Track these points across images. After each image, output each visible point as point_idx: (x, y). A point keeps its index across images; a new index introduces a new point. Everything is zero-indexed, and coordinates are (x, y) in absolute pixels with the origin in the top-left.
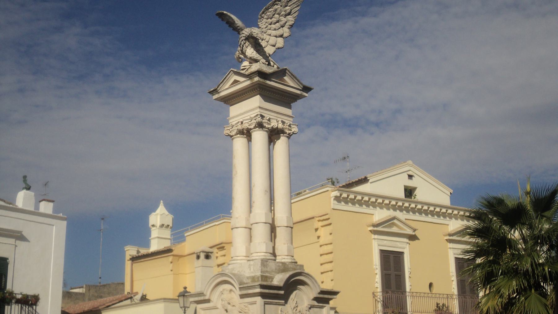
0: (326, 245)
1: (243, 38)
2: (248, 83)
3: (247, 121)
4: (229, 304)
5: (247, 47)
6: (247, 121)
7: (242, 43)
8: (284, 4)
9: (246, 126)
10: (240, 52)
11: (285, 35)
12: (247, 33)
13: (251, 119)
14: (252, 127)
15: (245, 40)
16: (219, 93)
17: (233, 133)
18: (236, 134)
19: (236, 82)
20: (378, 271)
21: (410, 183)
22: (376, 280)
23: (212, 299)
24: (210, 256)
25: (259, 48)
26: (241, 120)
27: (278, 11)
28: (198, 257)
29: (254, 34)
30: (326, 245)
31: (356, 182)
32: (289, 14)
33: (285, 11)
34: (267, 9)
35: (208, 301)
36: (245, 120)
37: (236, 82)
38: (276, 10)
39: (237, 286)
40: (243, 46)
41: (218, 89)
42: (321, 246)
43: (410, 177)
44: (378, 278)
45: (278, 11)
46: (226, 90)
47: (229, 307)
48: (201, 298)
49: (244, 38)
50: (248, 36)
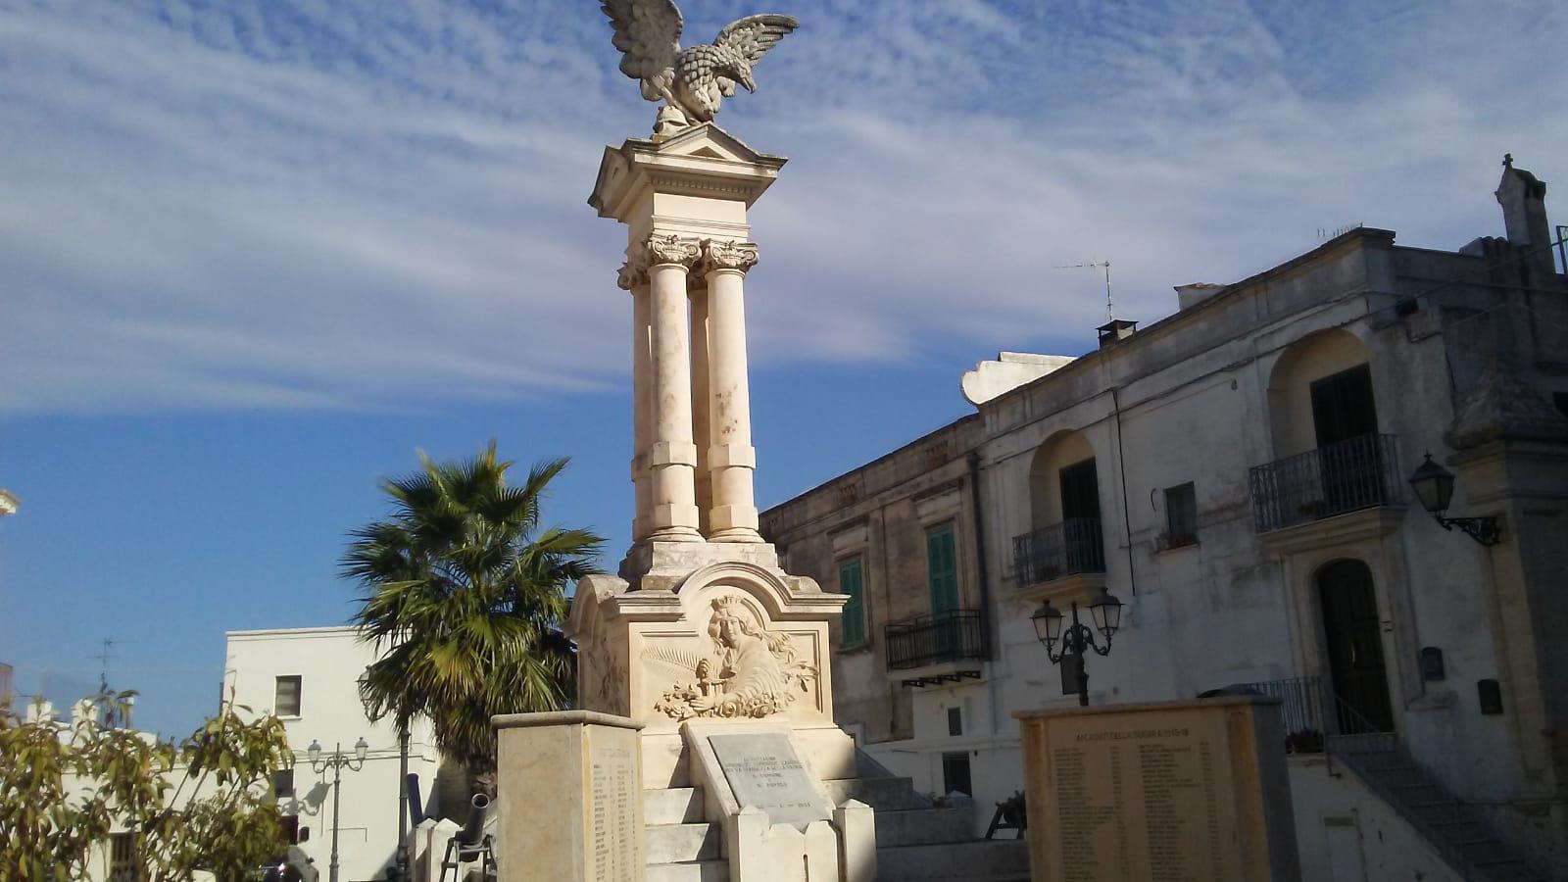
1: (708, 63)
2: (749, 171)
3: (718, 246)
4: (744, 630)
5: (703, 84)
6: (718, 246)
8: (758, 33)
9: (715, 250)
10: (671, 82)
11: (729, 92)
12: (724, 60)
13: (730, 246)
15: (711, 69)
18: (678, 262)
19: (705, 153)
23: (686, 615)
26: (704, 238)
27: (745, 42)
29: (741, 69)
32: (749, 57)
33: (751, 47)
34: (740, 27)
35: (675, 618)
36: (716, 242)
37: (705, 153)
38: (746, 37)
40: (698, 77)
45: (745, 42)
46: (678, 157)
47: (739, 638)
48: (666, 610)
49: (713, 65)
50: (725, 67)
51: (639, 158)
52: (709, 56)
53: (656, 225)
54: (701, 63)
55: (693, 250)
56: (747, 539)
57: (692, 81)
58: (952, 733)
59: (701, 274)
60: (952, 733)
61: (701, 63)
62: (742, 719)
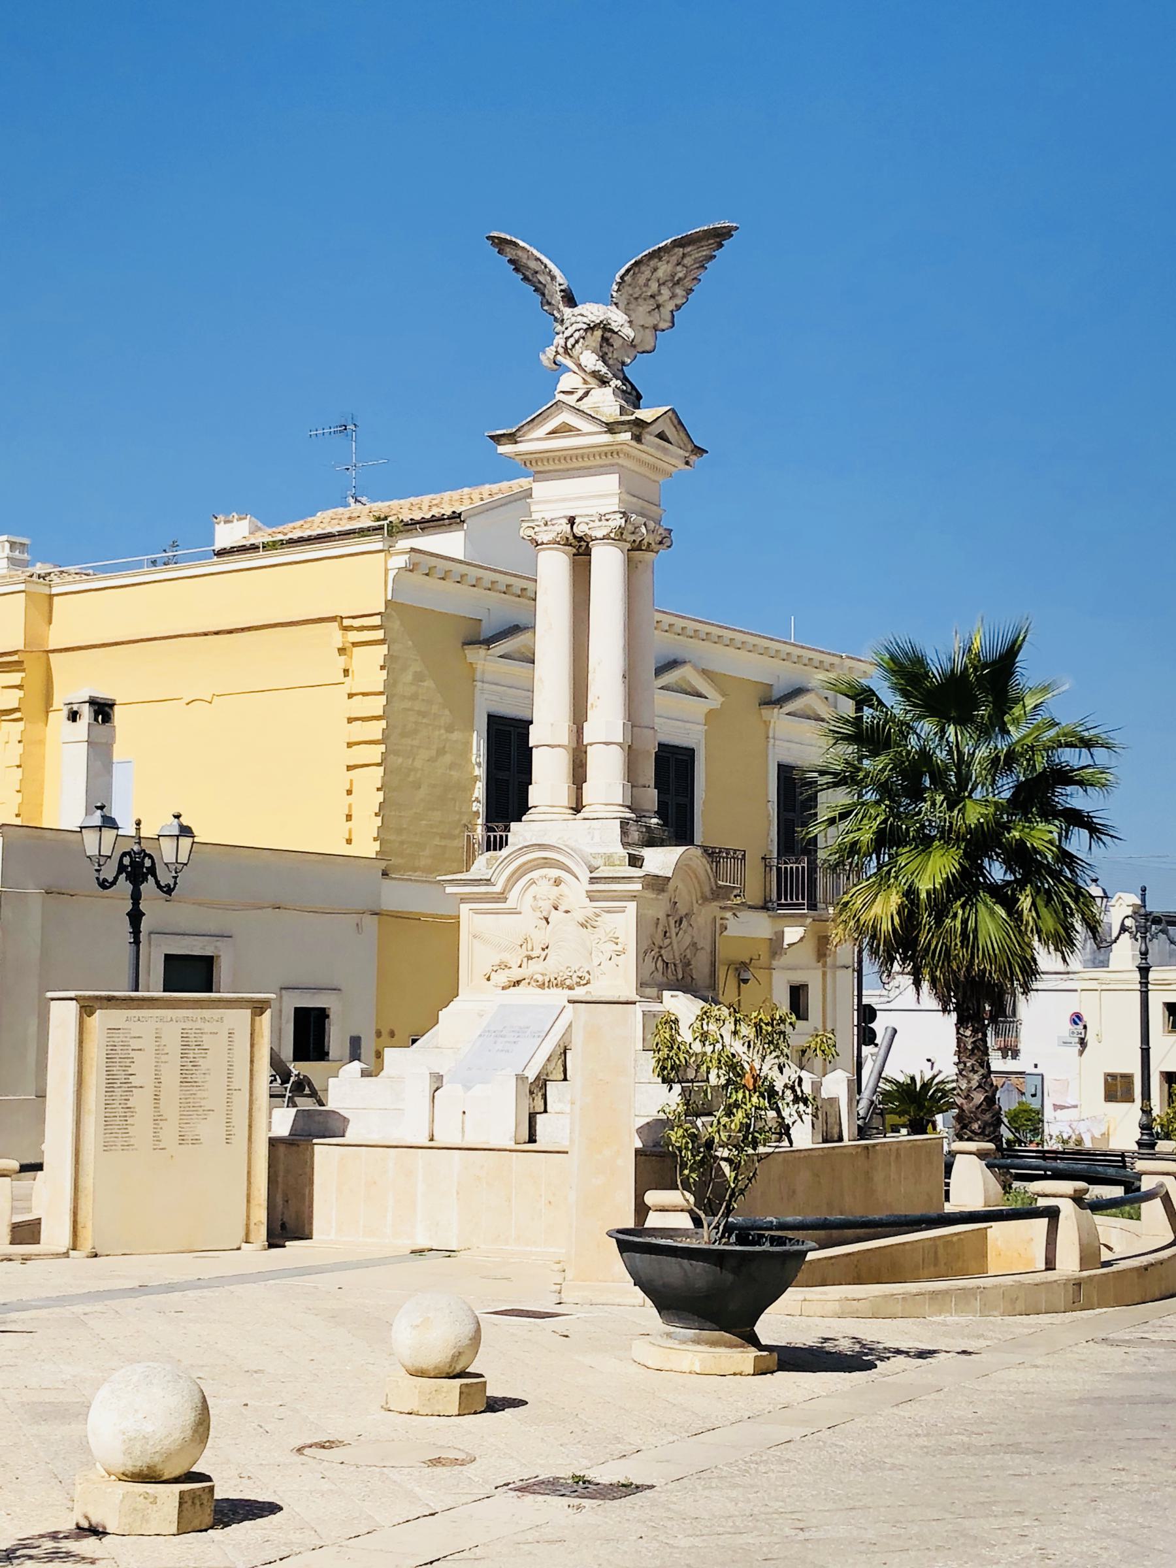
0: (364, 694)
7: (577, 335)
10: (561, 350)
14: (600, 535)
16: (516, 442)
17: (543, 537)
19: (565, 430)
20: (481, 772)
22: (476, 795)
25: (605, 349)
28: (74, 716)
29: (613, 324)
30: (364, 694)
31: (423, 521)
37: (565, 430)
39: (585, 875)
41: (519, 434)
42: (350, 696)
44: (480, 790)
49: (585, 326)
51: (501, 449)
52: (580, 318)
53: (533, 508)
54: (575, 327)
55: (558, 529)
56: (595, 815)
57: (573, 346)
58: (321, 1015)
59: (580, 550)
60: (321, 1015)
61: (575, 327)
62: (554, 990)
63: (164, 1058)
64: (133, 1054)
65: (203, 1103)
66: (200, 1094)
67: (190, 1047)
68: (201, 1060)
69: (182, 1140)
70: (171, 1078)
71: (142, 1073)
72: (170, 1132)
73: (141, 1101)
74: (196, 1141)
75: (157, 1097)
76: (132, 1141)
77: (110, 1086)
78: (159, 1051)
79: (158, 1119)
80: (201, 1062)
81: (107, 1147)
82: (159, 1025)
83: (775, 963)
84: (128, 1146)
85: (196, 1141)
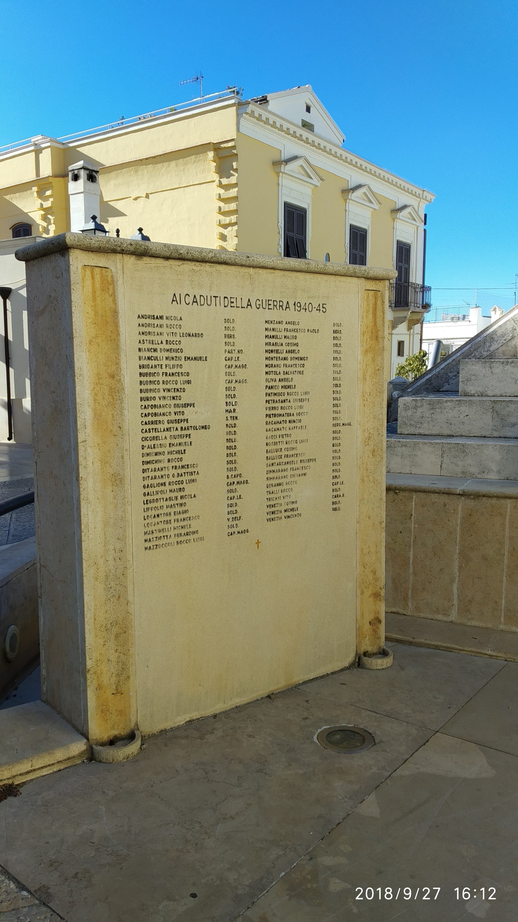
21: (308, 118)
24: (95, 177)
43: (308, 109)
63: (240, 374)
64: (187, 367)
65: (300, 448)
66: (297, 434)
67: (281, 352)
68: (296, 377)
69: (273, 515)
70: (252, 405)
71: (206, 404)
72: (253, 499)
73: (206, 453)
74: (292, 512)
75: (231, 448)
76: (195, 525)
77: (150, 422)
78: (234, 361)
79: (235, 481)
80: (296, 379)
81: (152, 542)
82: (230, 313)
83: (393, 332)
84: (187, 535)
85: (292, 512)
